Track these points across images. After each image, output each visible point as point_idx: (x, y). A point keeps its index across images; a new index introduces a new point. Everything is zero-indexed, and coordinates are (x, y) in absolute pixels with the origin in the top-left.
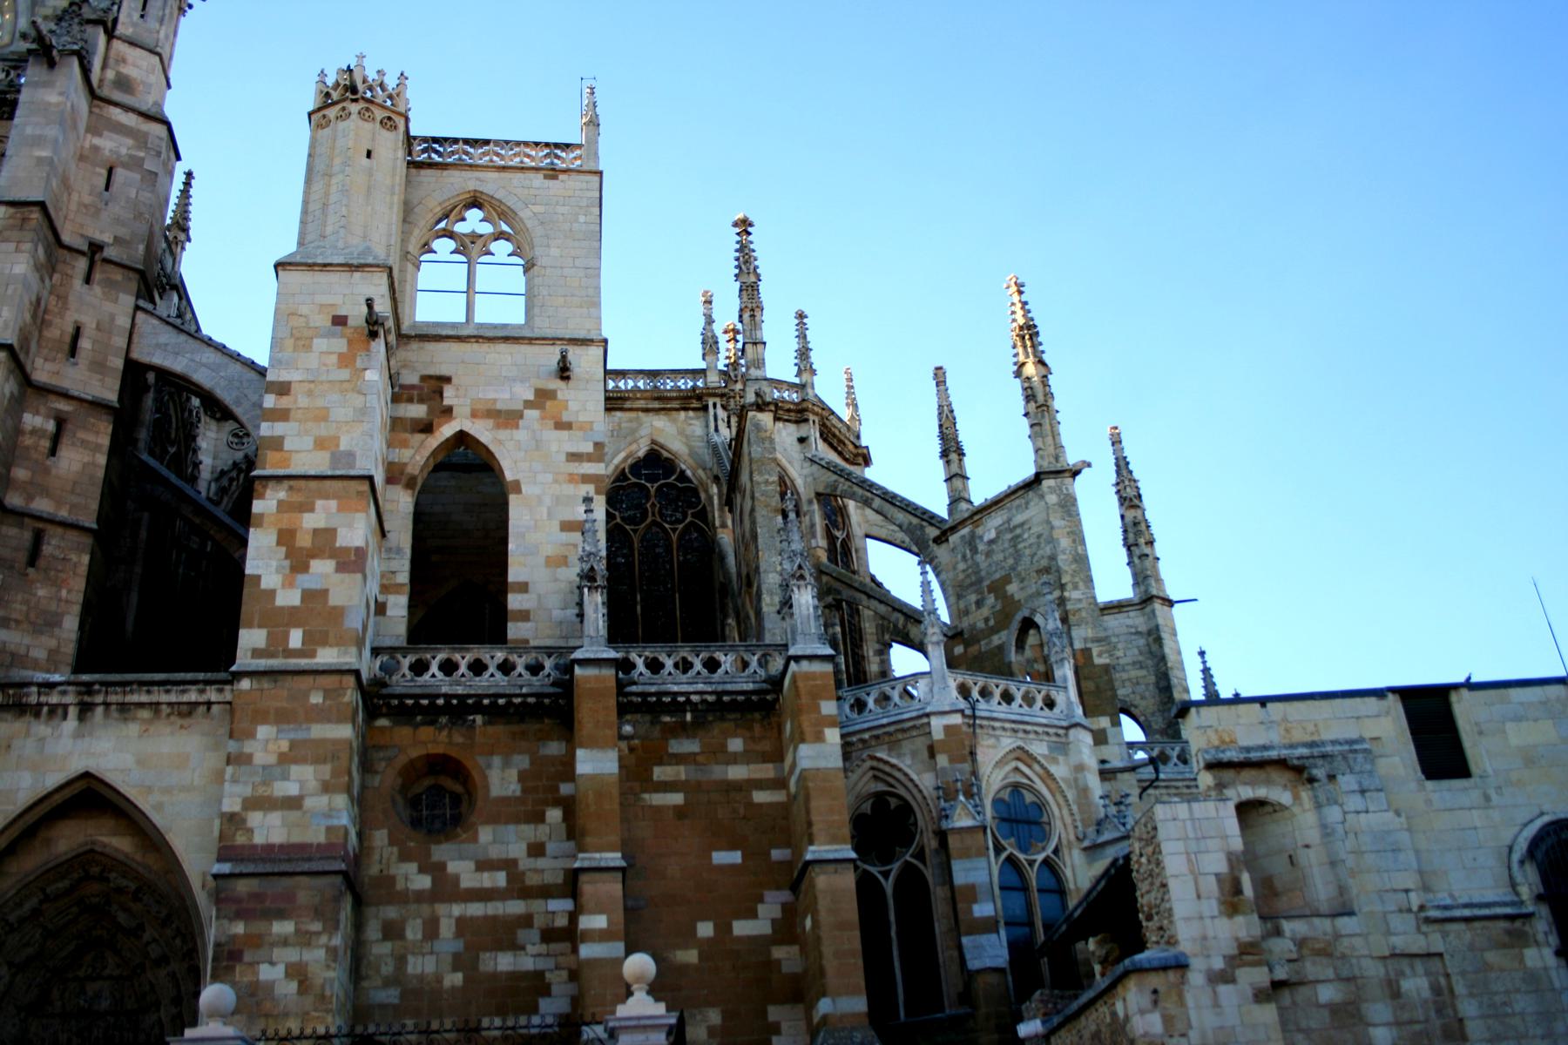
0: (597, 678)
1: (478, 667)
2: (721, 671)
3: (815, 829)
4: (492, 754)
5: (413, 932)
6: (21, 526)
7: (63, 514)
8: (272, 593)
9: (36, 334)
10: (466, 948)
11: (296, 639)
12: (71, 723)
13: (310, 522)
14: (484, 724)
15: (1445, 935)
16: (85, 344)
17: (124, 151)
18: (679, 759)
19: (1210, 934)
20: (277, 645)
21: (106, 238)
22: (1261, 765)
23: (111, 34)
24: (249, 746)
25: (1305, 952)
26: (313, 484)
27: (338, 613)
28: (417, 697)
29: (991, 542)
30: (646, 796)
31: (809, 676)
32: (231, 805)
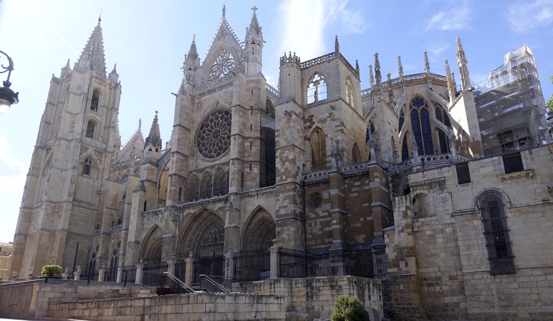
0: (333, 175)
2: (363, 167)
3: (373, 200)
4: (324, 190)
5: (313, 225)
7: (254, 159)
11: (284, 177)
12: (256, 197)
13: (285, 155)
14: (323, 185)
16: (253, 127)
17: (254, 85)
20: (281, 180)
21: (254, 105)
22: (422, 185)
24: (279, 198)
25: (424, 224)
26: (284, 148)
27: (290, 171)
31: (372, 168)
32: (277, 208)
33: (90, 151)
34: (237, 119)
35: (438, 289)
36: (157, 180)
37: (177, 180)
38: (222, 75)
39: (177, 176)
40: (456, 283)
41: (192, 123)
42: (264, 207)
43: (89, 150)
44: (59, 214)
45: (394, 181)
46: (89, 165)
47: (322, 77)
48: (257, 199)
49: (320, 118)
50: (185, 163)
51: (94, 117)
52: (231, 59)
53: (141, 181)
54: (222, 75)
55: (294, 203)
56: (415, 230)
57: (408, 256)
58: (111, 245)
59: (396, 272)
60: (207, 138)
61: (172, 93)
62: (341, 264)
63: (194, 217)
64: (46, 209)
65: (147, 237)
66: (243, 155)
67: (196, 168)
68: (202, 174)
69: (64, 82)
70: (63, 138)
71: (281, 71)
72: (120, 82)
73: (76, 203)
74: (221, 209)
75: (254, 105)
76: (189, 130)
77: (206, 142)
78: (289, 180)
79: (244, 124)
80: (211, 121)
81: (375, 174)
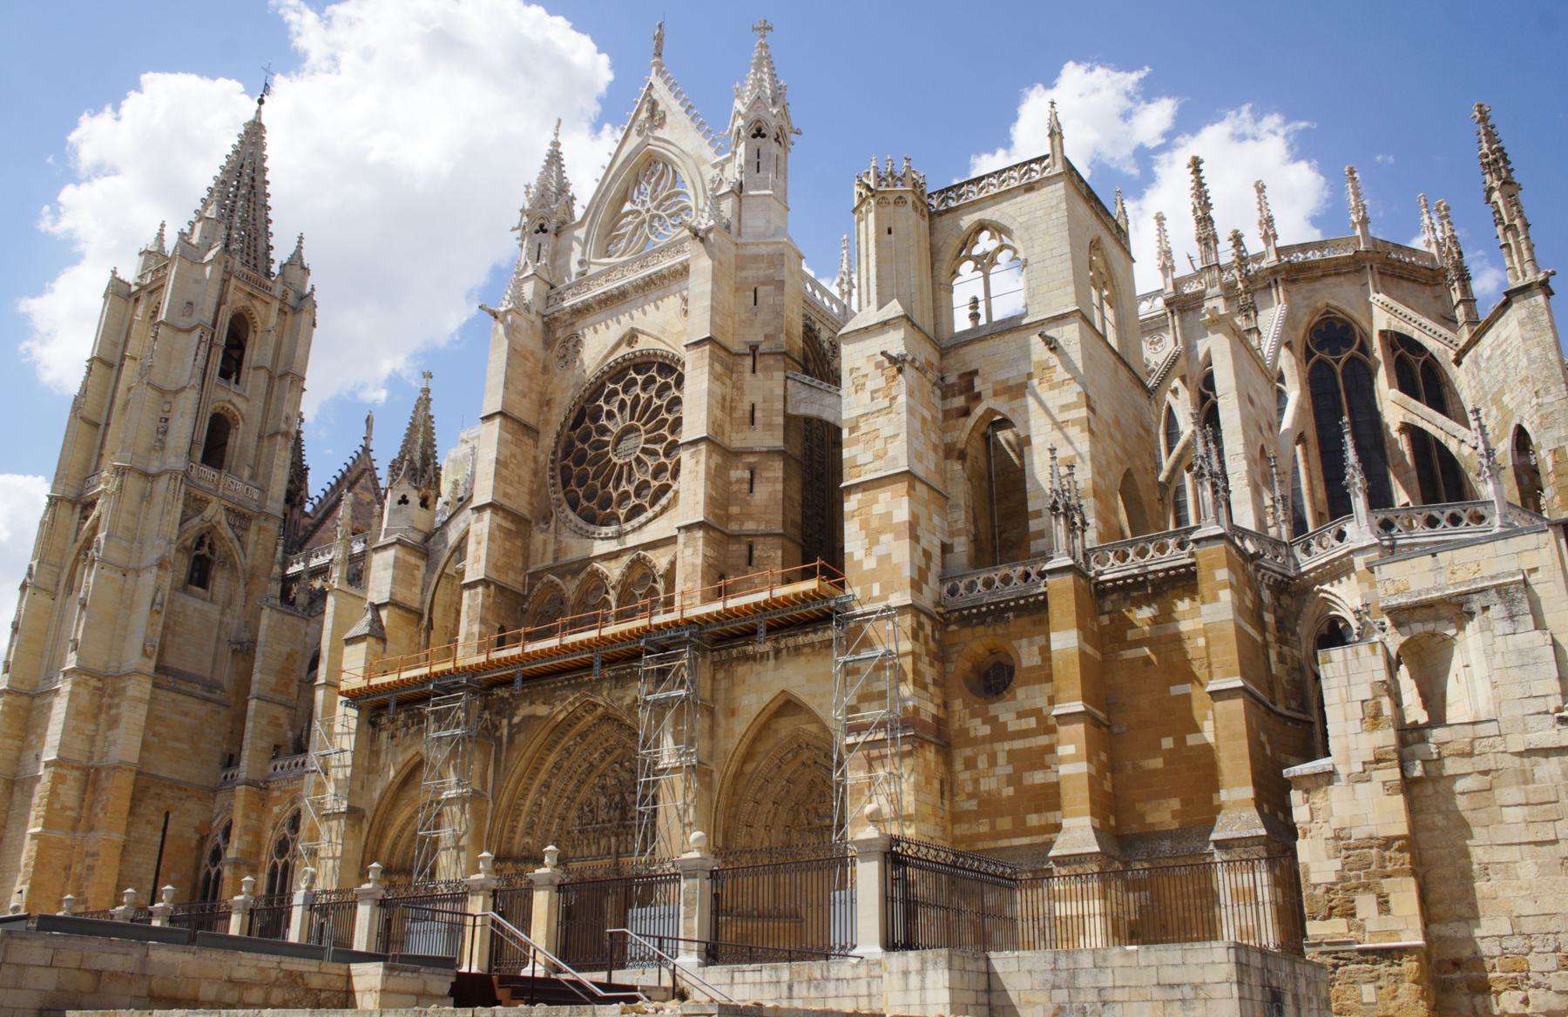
1: (1006, 580)
4: (1021, 638)
5: (982, 763)
6: (739, 542)
8: (860, 562)
9: (728, 418)
10: (1015, 771)
11: (876, 590)
12: (772, 662)
13: (878, 509)
14: (1015, 617)
16: (758, 414)
17: (761, 273)
19: (1353, 746)
21: (760, 338)
28: (960, 610)
29: (1489, 358)
36: (423, 603)
37: (491, 600)
39: (492, 587)
41: (545, 409)
42: (802, 693)
44: (113, 712)
45: (1280, 605)
46: (208, 555)
49: (1002, 381)
50: (519, 543)
51: (230, 401)
53: (372, 604)
58: (269, 824)
59: (1342, 935)
60: (595, 456)
62: (1096, 906)
64: (73, 696)
65: (389, 795)
67: (556, 559)
68: (577, 582)
69: (143, 294)
72: (313, 289)
73: (163, 679)
77: (591, 471)
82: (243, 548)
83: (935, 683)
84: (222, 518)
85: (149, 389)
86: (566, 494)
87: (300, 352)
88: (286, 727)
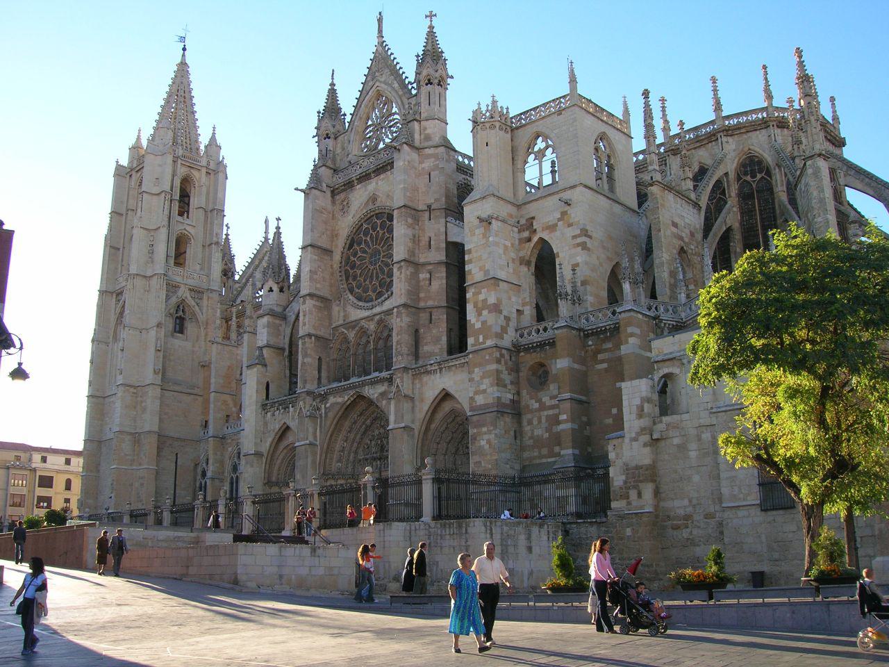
3: (625, 377)
5: (535, 422)
11: (481, 340)
12: (438, 374)
13: (481, 297)
15: (717, 417)
18: (606, 350)
20: (477, 340)
21: (432, 201)
23: (419, 121)
24: (473, 376)
26: (480, 284)
30: (596, 366)
33: (183, 292)
34: (403, 232)
35: (685, 534)
37: (313, 345)
38: (381, 146)
39: (313, 338)
40: (712, 522)
42: (452, 391)
43: (180, 291)
44: (143, 405)
47: (550, 143)
48: (440, 378)
51: (185, 229)
52: (394, 114)
53: (259, 347)
54: (381, 146)
55: (498, 385)
56: (655, 437)
57: (641, 482)
61: (296, 189)
62: (572, 491)
63: (343, 410)
66: (415, 297)
67: (344, 321)
68: (354, 332)
69: (134, 173)
70: (137, 274)
71: (474, 137)
72: (223, 158)
74: (383, 394)
75: (432, 201)
76: (328, 252)
77: (359, 272)
78: (489, 343)
79: (415, 240)
80: (365, 235)
81: (630, 330)
82: (200, 309)
83: (512, 383)
84: (188, 294)
85: (142, 230)
86: (347, 285)
87: (219, 195)
88: (231, 405)
